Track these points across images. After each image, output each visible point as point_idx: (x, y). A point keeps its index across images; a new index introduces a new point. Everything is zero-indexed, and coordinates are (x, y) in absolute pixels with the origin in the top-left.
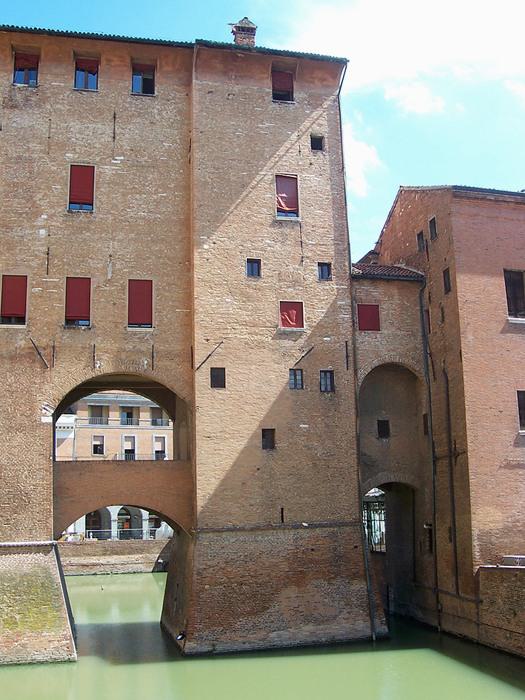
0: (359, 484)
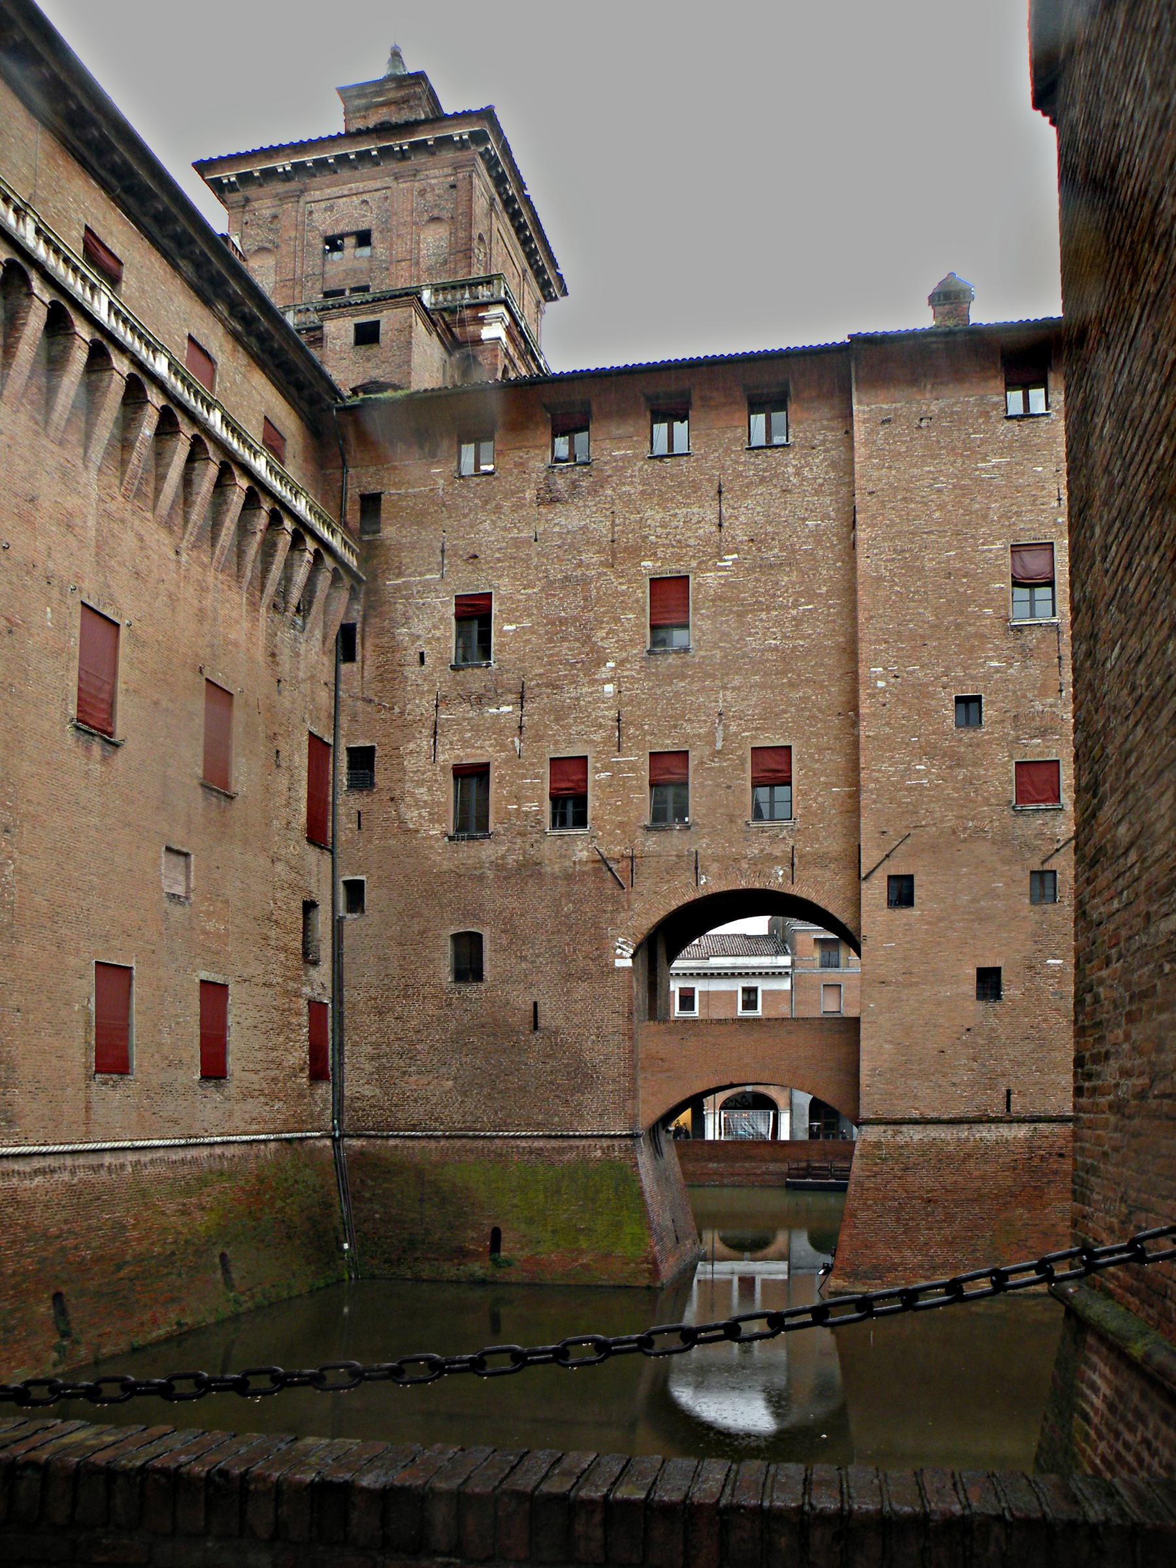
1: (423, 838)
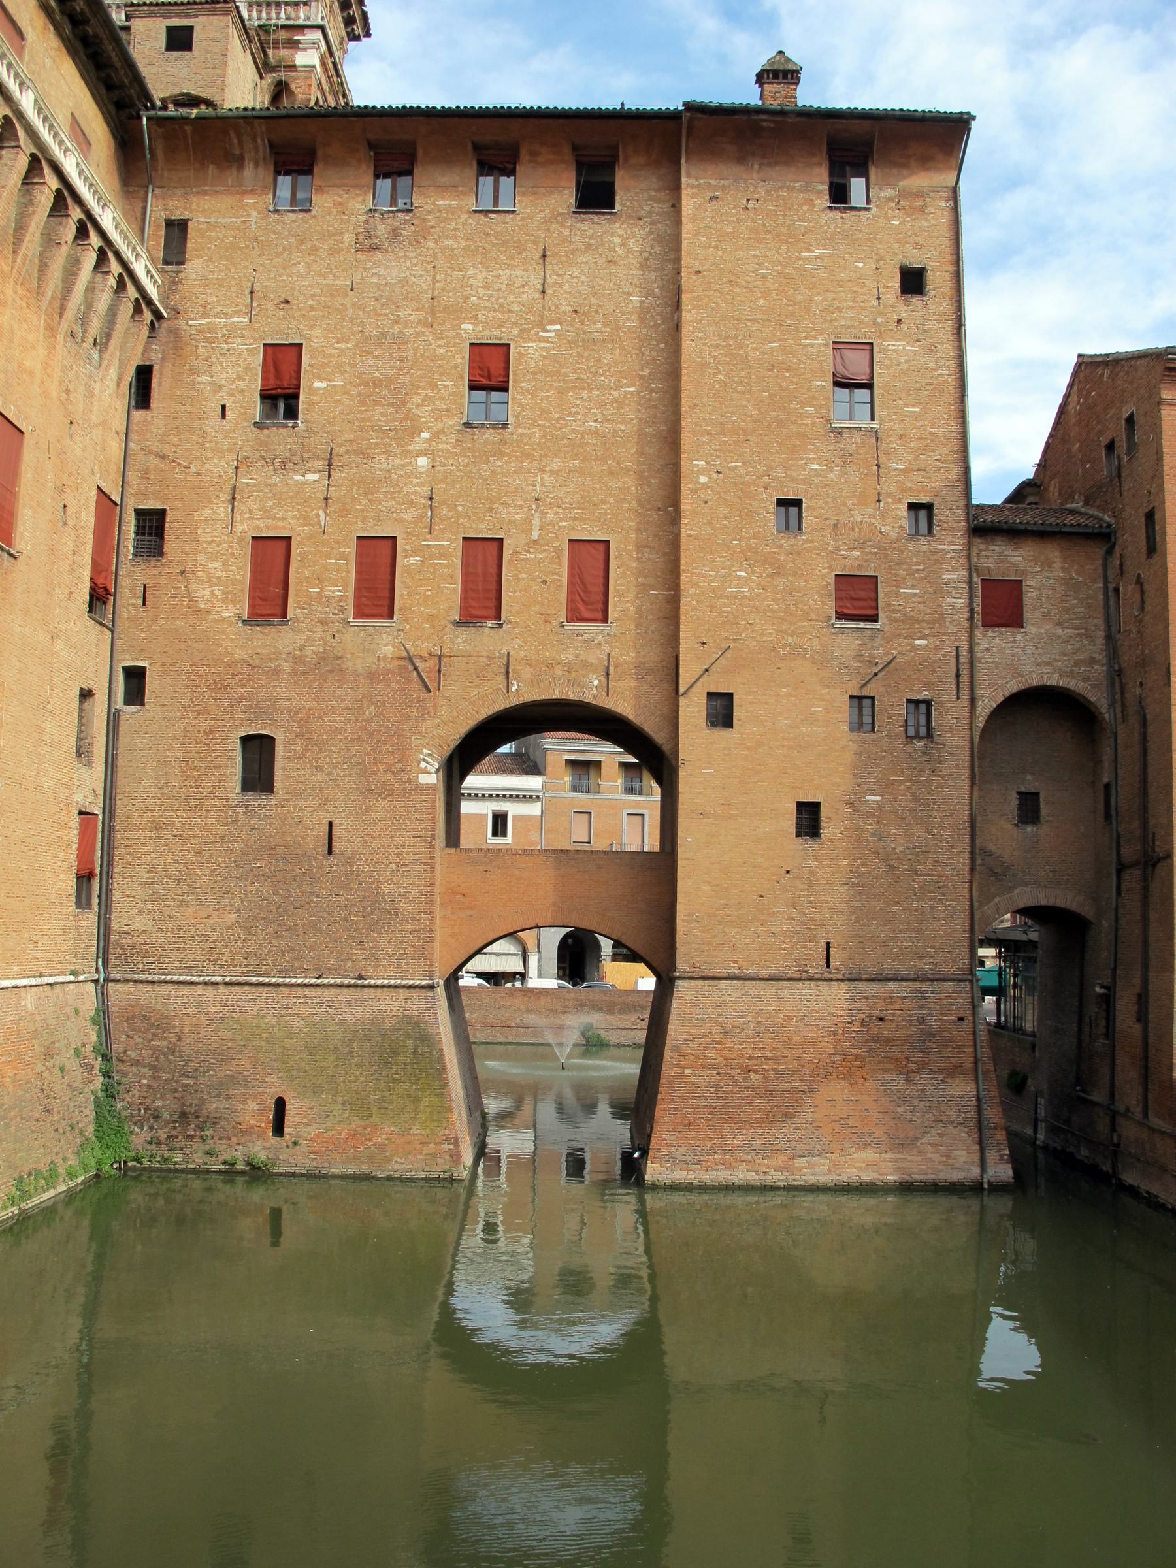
0: (972, 906)
1: (215, 621)
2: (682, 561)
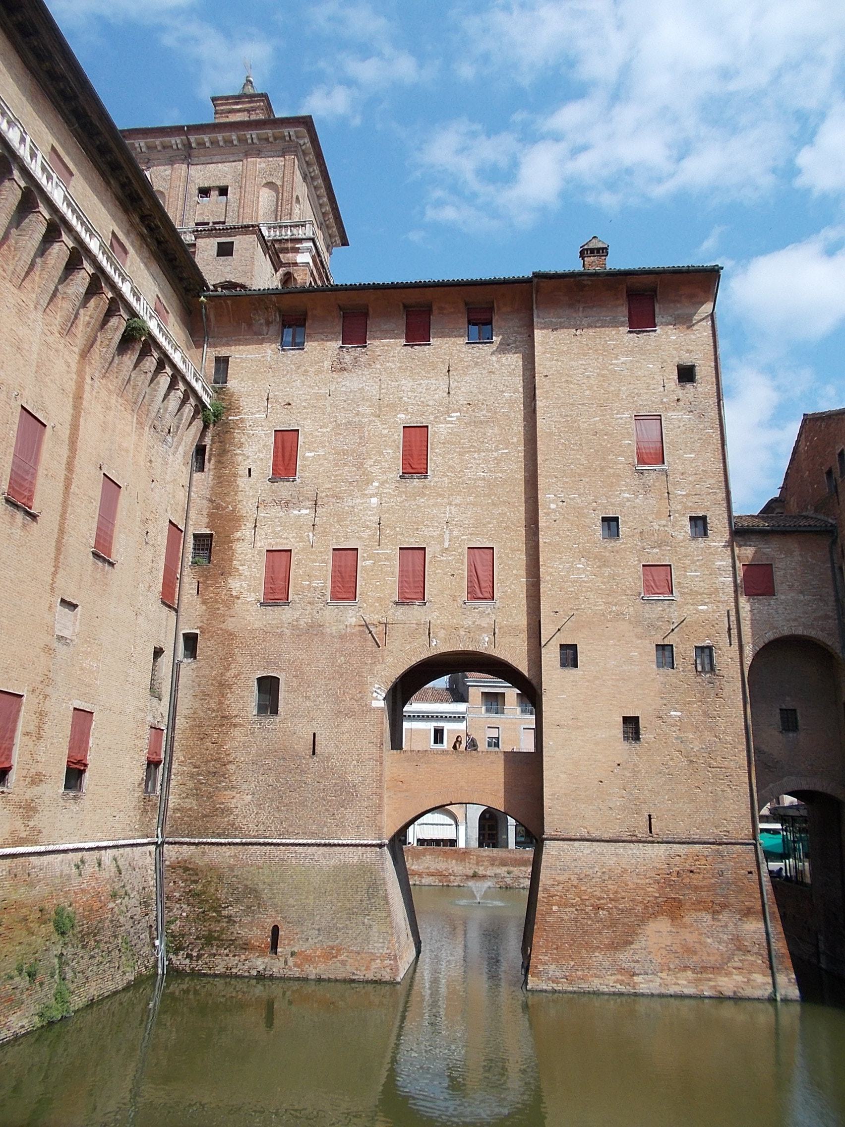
1: (242, 604)
2: (541, 559)
